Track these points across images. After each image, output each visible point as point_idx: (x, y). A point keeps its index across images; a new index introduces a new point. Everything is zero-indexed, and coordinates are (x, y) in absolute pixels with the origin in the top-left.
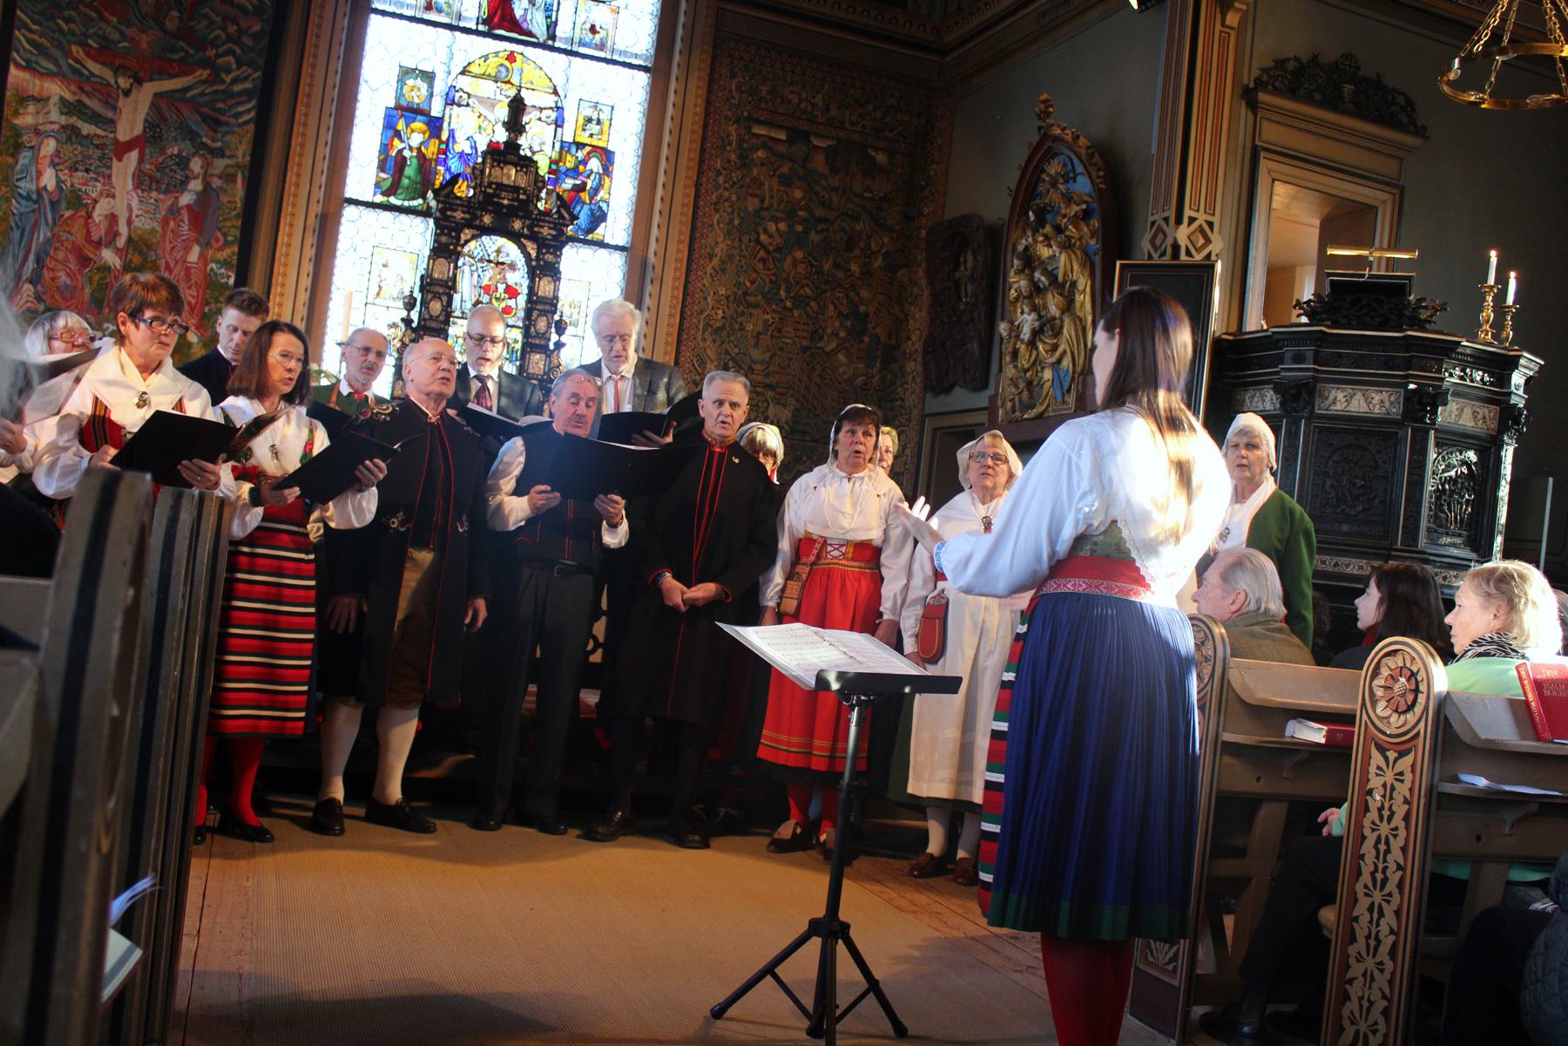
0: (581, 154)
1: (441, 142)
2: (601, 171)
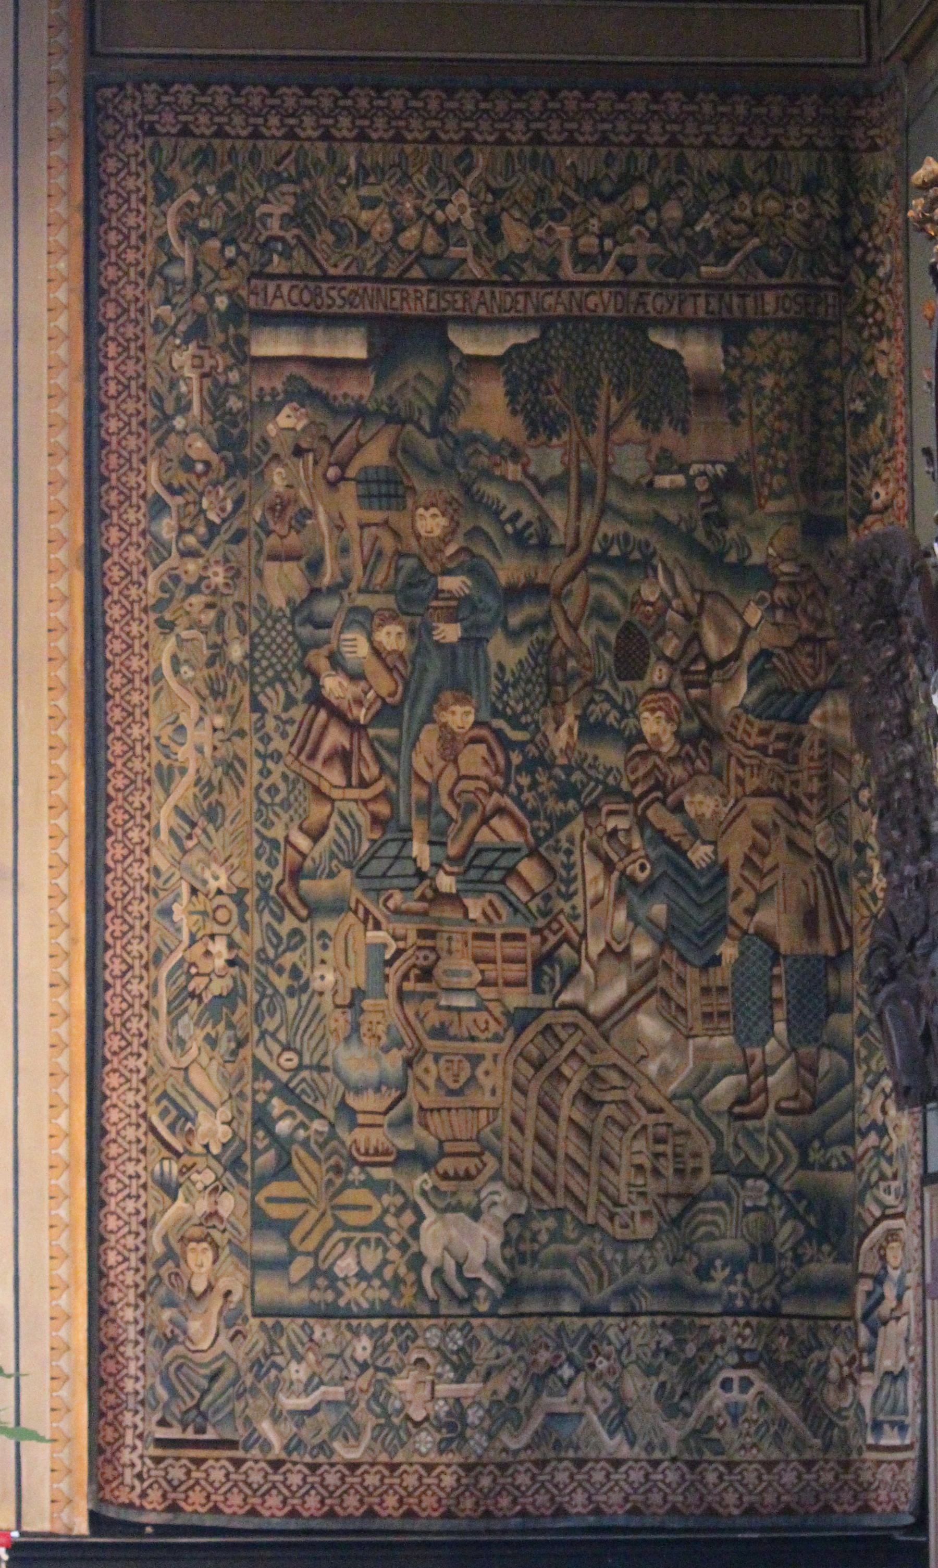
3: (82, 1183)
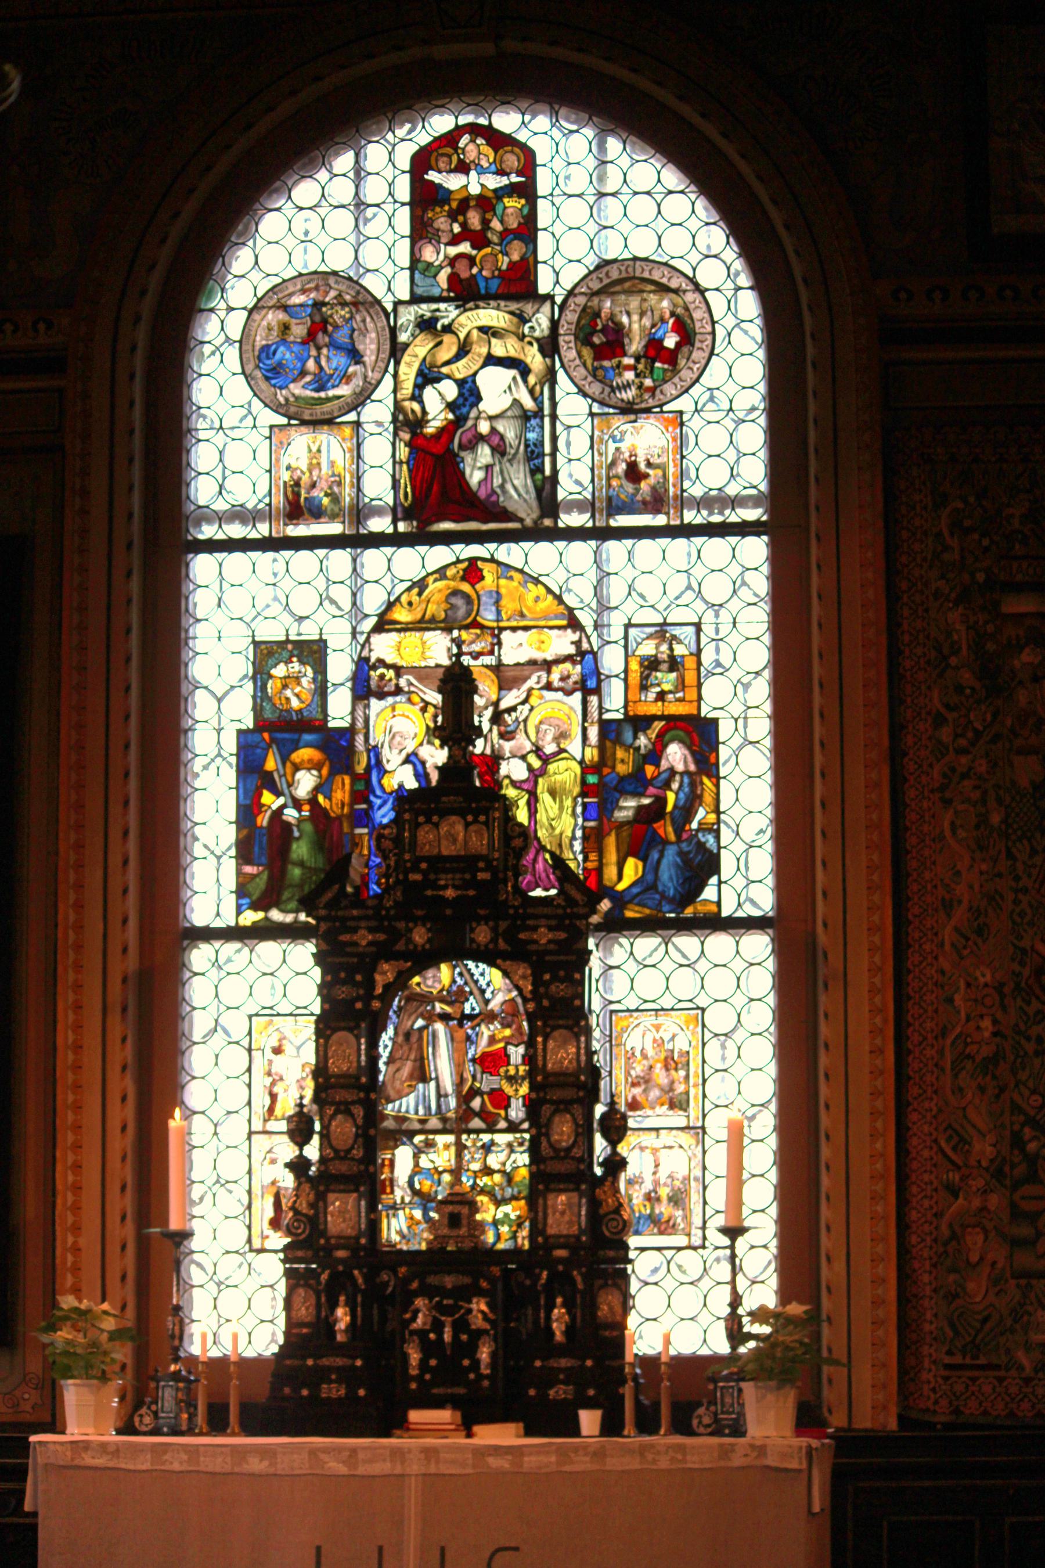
0: (642, 741)
1: (355, 778)
2: (692, 768)
3: (893, 1188)
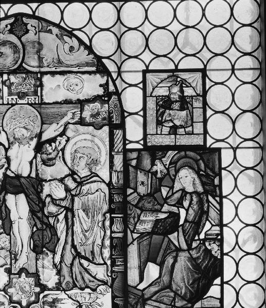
0: (159, 167)
2: (200, 189)
